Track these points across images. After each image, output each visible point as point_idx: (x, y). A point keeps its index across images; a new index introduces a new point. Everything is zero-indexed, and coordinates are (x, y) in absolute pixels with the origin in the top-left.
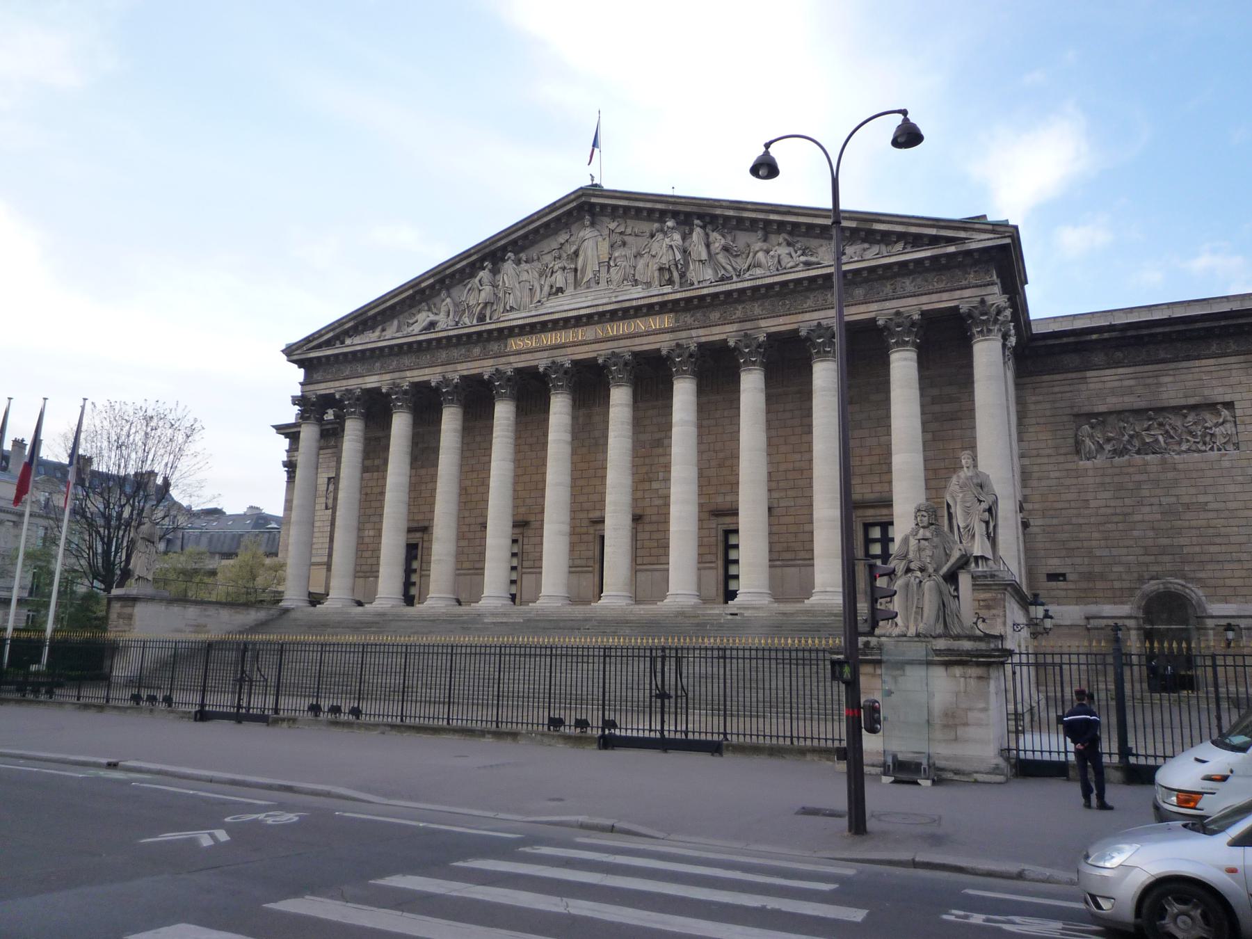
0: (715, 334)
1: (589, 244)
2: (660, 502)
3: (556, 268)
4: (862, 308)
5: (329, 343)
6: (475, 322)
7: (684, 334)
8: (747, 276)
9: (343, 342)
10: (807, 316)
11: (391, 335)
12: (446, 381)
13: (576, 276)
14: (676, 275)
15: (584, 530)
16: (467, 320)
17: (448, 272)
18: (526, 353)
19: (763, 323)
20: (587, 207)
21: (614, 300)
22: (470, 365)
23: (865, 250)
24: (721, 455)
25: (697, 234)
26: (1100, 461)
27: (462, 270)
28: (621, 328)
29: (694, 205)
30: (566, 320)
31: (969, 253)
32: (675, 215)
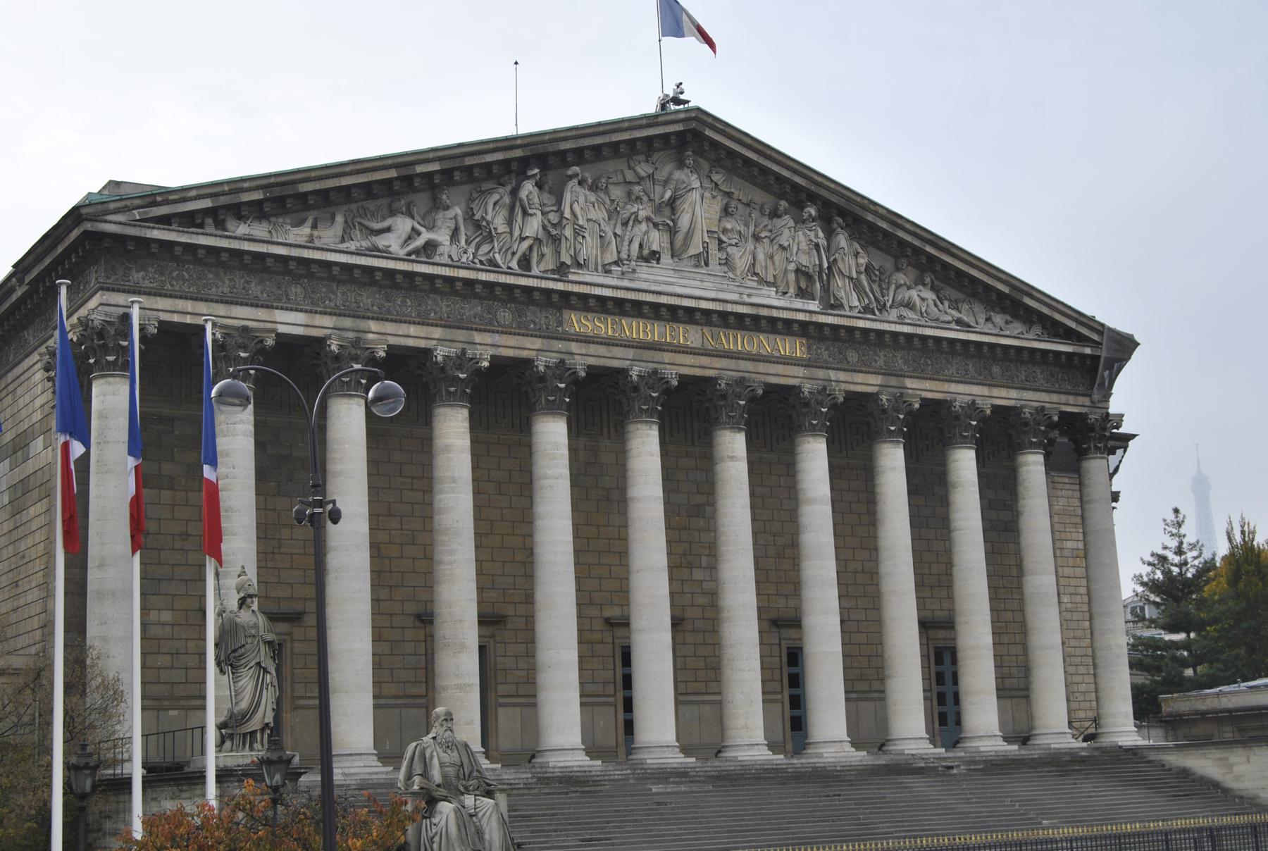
0: (867, 383)
1: (695, 196)
2: (701, 600)
3: (642, 214)
4: (1003, 392)
5: (191, 220)
6: (514, 264)
7: (821, 373)
8: (894, 314)
9: (220, 224)
10: (953, 387)
11: (327, 242)
12: (461, 360)
13: (672, 243)
14: (818, 285)
15: (597, 636)
16: (498, 257)
17: (469, 161)
19: (910, 383)
20: (686, 138)
21: (747, 300)
22: (497, 338)
23: (1007, 322)
24: (780, 540)
27: (487, 167)
29: (843, 196)
30: (673, 309)
31: (1096, 359)
32: (812, 197)
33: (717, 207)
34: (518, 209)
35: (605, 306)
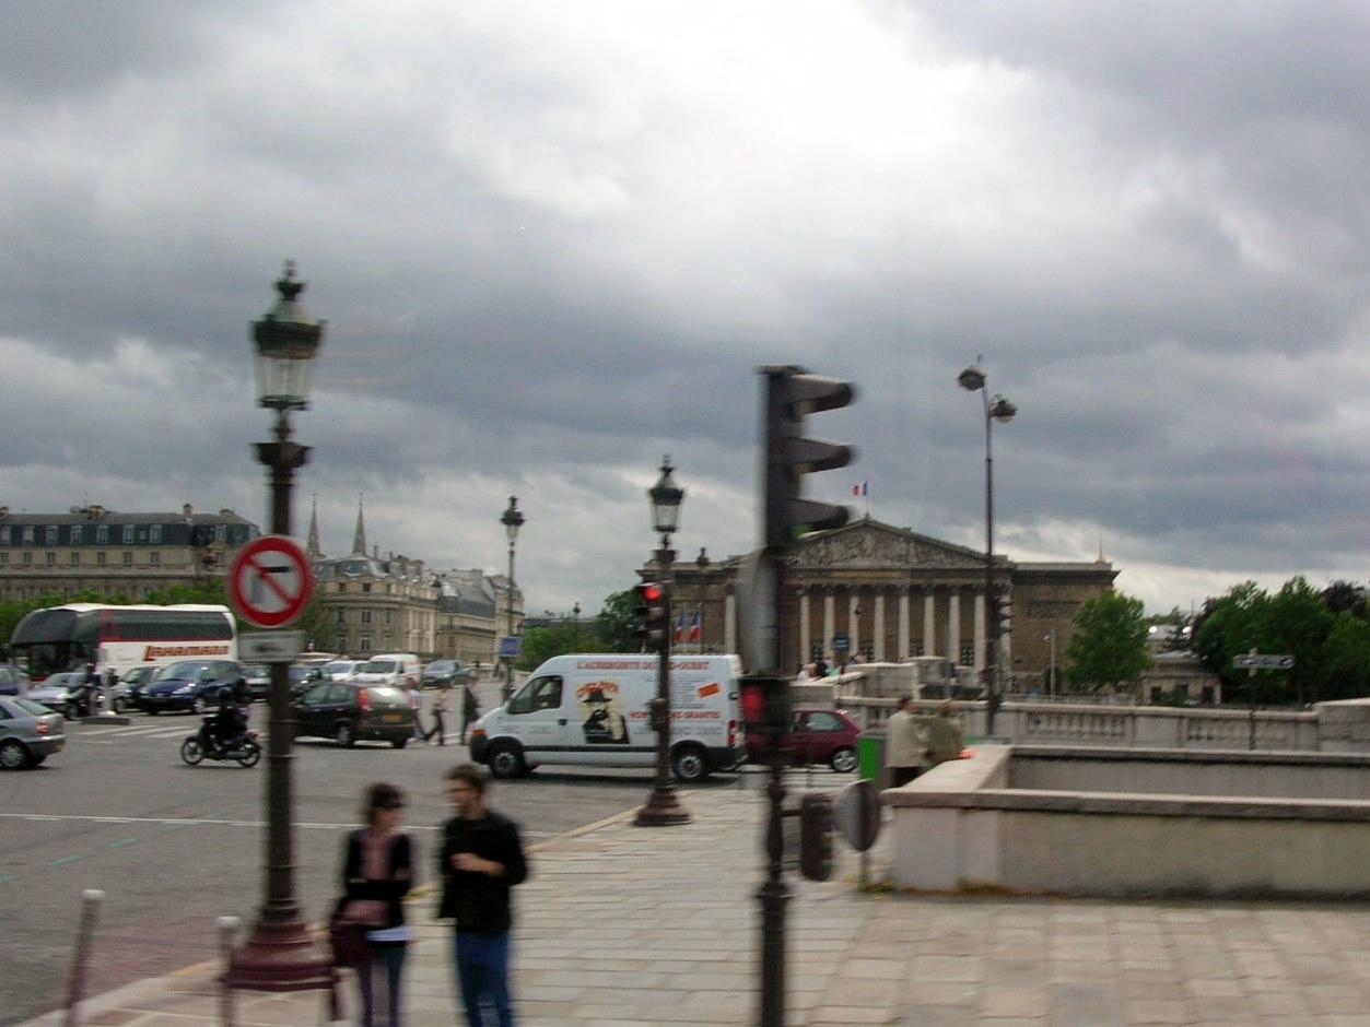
18: (837, 579)
25: (912, 545)
26: (1035, 620)
28: (879, 574)
33: (874, 543)
34: (819, 551)
35: (838, 570)
